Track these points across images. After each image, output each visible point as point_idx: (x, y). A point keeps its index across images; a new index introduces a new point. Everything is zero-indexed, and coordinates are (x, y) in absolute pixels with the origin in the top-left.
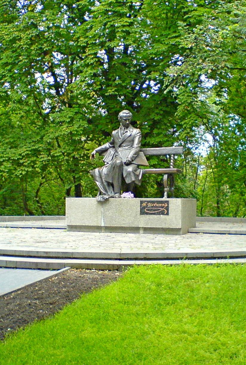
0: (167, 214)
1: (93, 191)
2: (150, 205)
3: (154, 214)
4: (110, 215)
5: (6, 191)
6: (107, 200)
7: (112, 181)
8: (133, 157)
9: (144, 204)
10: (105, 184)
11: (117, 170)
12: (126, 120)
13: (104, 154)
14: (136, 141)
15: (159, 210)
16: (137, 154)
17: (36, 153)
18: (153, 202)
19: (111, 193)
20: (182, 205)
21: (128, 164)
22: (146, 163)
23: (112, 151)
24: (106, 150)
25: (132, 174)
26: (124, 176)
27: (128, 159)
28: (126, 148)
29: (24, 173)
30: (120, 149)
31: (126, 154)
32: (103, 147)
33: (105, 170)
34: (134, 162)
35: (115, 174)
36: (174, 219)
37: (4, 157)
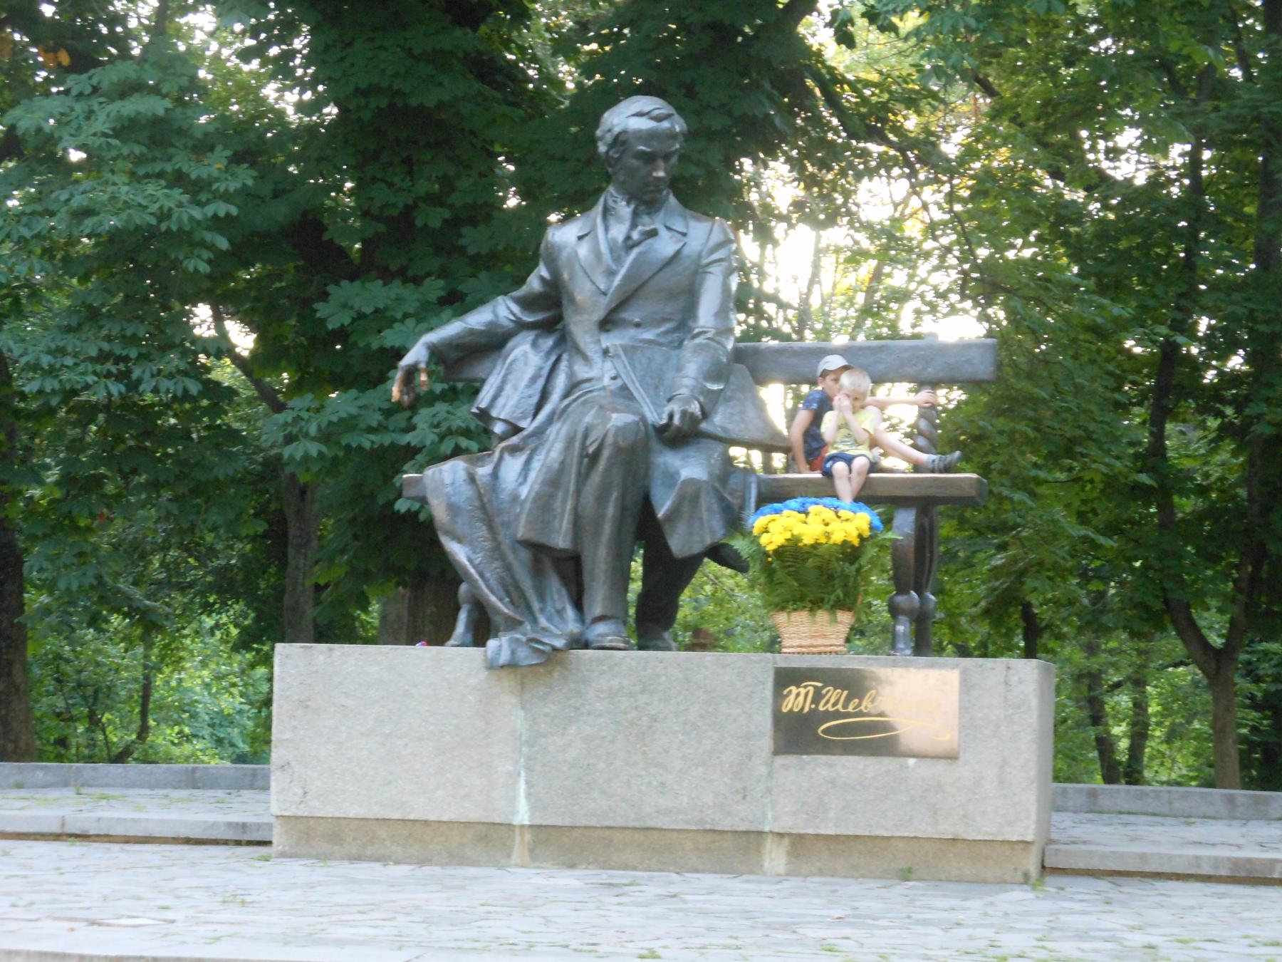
10: (520, 562)
12: (649, 158)
13: (478, 371)
19: (558, 623)
23: (526, 356)
24: (492, 344)
25: (707, 502)
26: (660, 514)
27: (676, 407)
28: (649, 335)
32: (478, 319)
33: (518, 477)
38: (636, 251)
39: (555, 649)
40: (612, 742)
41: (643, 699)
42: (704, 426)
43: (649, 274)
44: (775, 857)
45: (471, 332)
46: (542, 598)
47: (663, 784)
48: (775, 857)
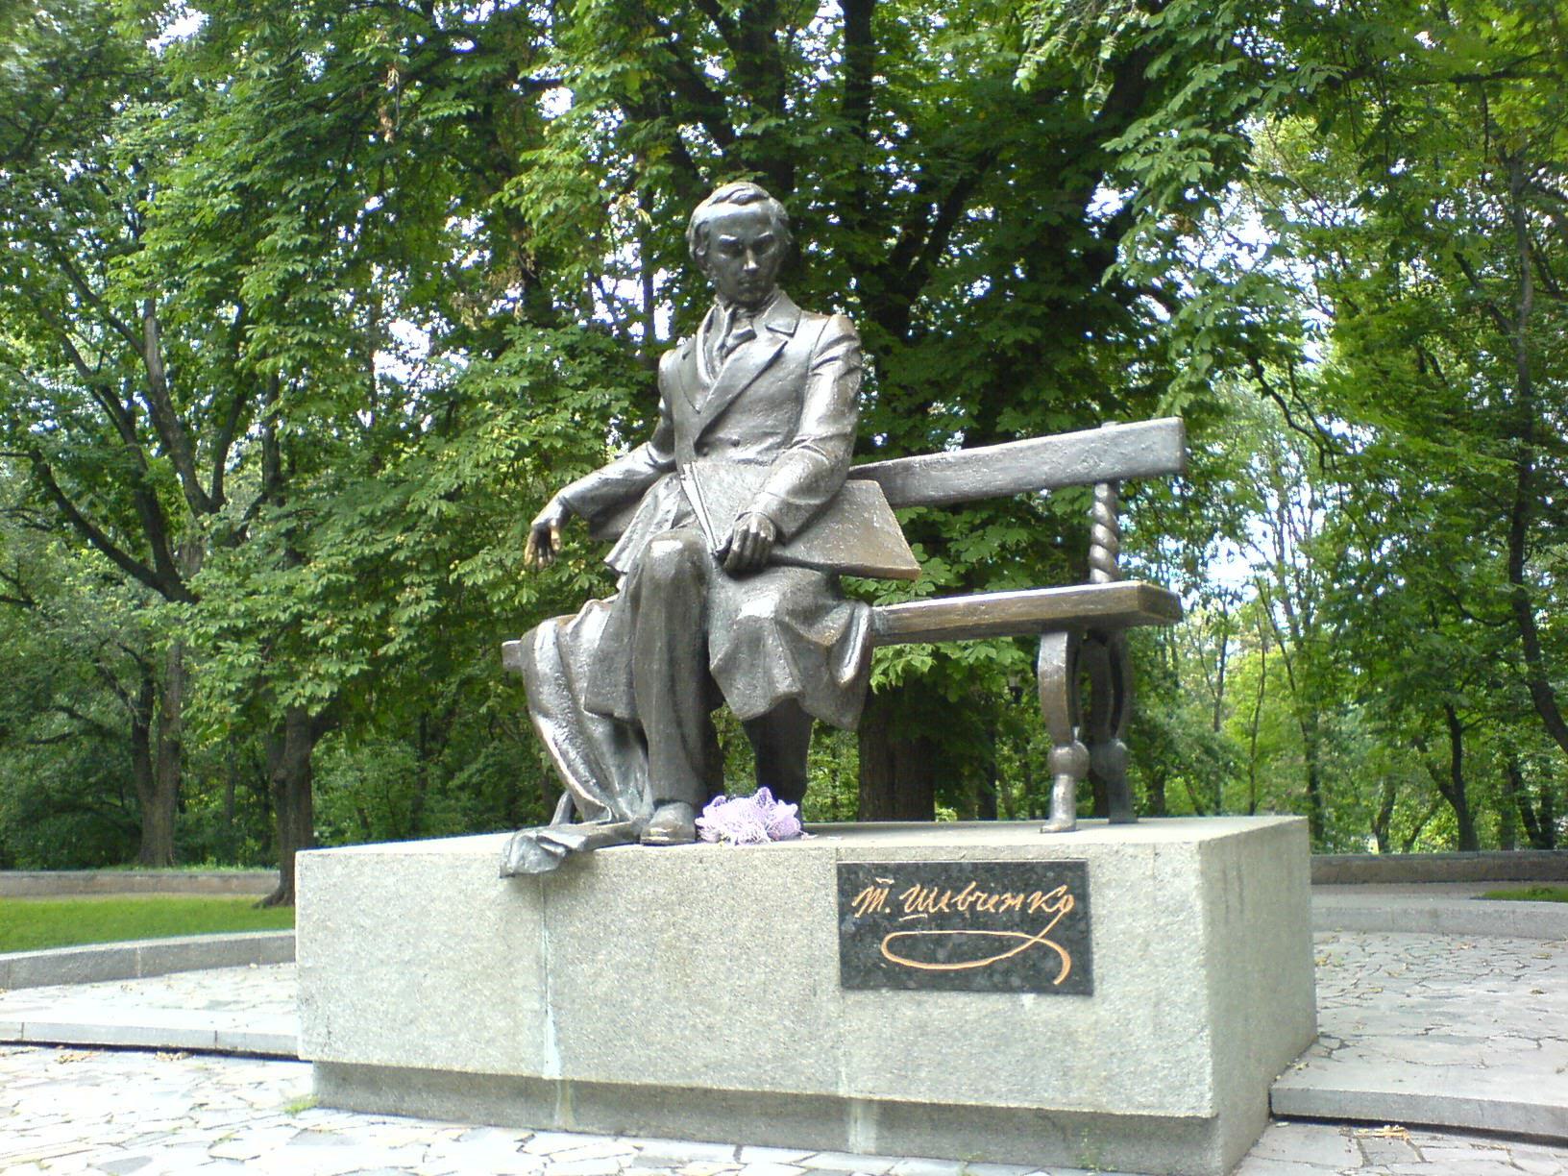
0: (1081, 984)
1: (517, 795)
2: (919, 901)
3: (962, 983)
4: (602, 987)
5: (480, 771)
6: (573, 865)
7: (632, 704)
8: (787, 507)
9: (873, 898)
11: (658, 619)
12: (736, 250)
14: (822, 396)
15: (1004, 945)
16: (822, 501)
17: (375, 578)
18: (945, 876)
20: (1211, 904)
21: (750, 562)
22: (903, 556)
25: (773, 643)
26: (714, 663)
28: (751, 452)
29: (326, 690)
30: (702, 464)
31: (735, 491)
34: (798, 551)
35: (647, 652)
36: (1141, 1035)
37: (225, 615)
38: (732, 357)
39: (569, 850)
40: (649, 971)
41: (683, 912)
42: (778, 552)
43: (746, 382)
44: (862, 1134)
45: (606, 482)
46: (625, 778)
47: (710, 1028)
48: (862, 1134)
